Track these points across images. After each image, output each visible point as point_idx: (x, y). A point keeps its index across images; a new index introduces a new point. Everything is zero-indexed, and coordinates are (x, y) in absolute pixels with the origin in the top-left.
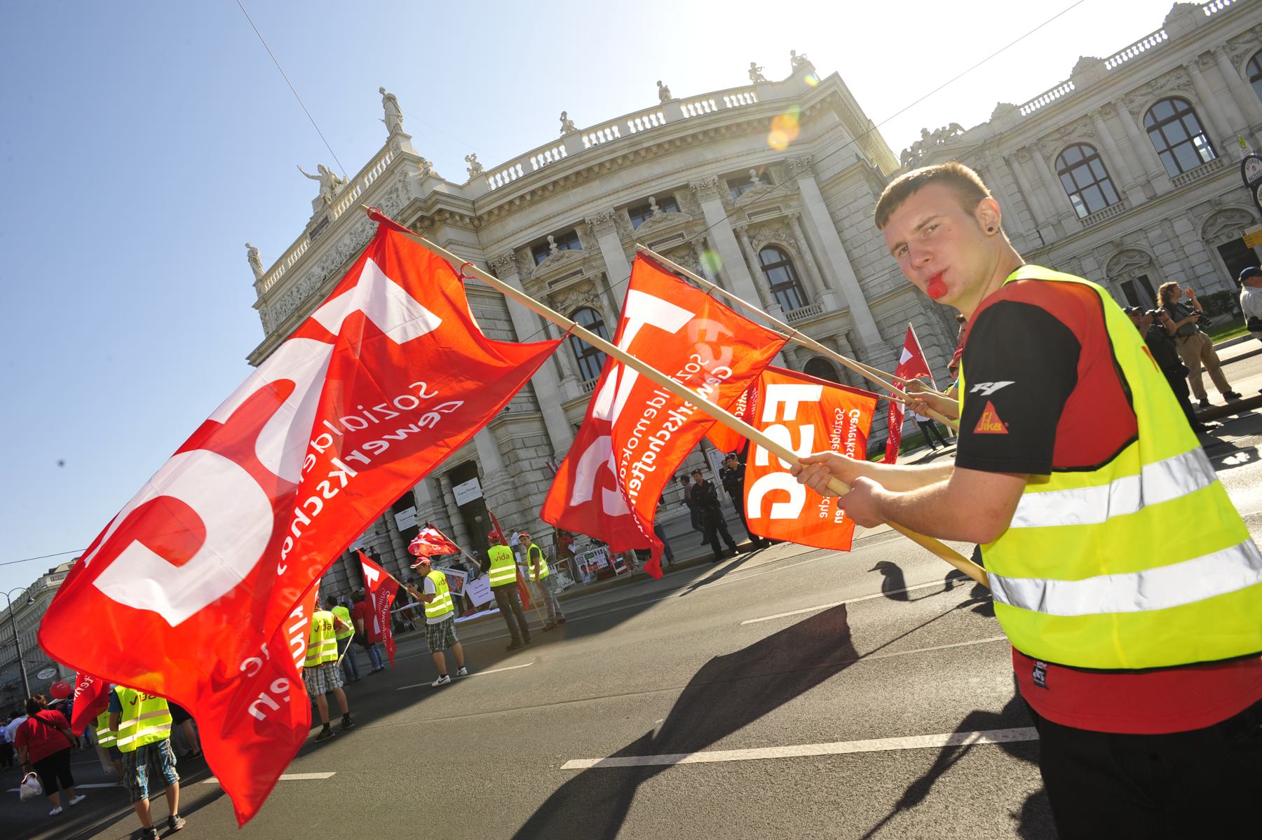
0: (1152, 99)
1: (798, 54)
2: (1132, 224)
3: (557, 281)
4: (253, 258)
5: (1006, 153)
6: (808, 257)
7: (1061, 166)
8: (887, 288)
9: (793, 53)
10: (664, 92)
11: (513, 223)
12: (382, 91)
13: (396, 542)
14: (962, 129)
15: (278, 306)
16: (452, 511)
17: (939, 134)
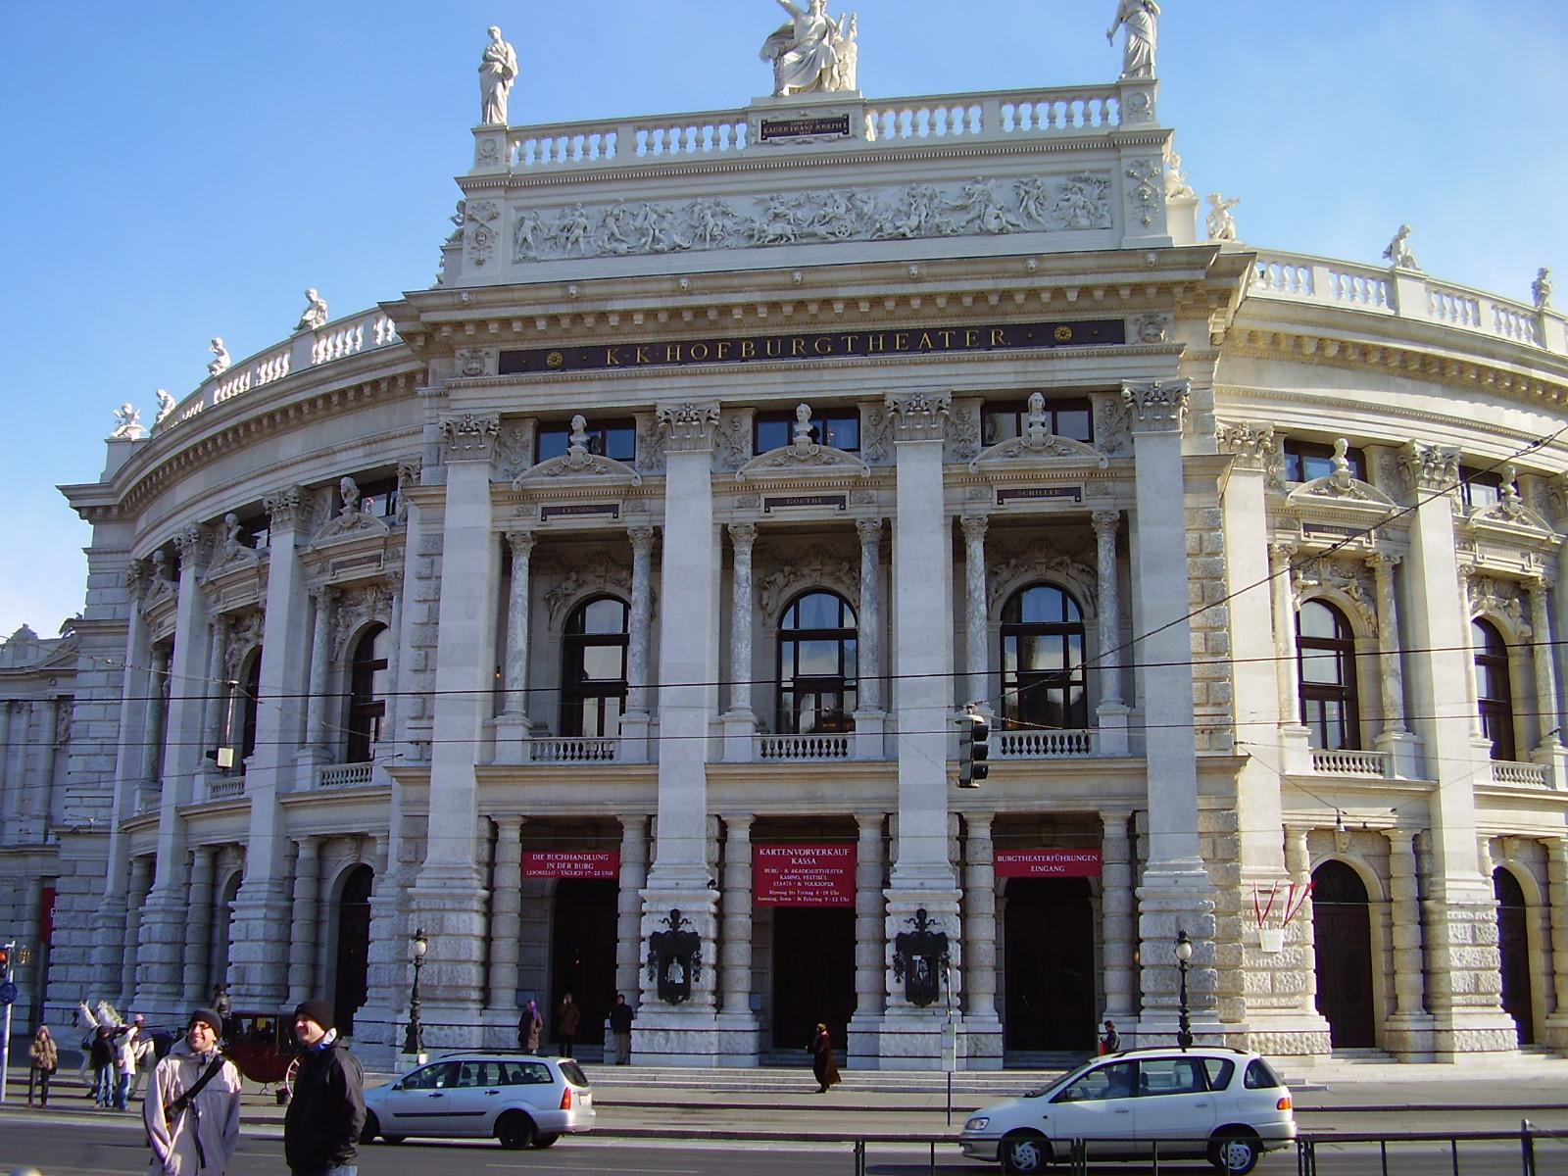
13: (741, 921)
15: (550, 220)
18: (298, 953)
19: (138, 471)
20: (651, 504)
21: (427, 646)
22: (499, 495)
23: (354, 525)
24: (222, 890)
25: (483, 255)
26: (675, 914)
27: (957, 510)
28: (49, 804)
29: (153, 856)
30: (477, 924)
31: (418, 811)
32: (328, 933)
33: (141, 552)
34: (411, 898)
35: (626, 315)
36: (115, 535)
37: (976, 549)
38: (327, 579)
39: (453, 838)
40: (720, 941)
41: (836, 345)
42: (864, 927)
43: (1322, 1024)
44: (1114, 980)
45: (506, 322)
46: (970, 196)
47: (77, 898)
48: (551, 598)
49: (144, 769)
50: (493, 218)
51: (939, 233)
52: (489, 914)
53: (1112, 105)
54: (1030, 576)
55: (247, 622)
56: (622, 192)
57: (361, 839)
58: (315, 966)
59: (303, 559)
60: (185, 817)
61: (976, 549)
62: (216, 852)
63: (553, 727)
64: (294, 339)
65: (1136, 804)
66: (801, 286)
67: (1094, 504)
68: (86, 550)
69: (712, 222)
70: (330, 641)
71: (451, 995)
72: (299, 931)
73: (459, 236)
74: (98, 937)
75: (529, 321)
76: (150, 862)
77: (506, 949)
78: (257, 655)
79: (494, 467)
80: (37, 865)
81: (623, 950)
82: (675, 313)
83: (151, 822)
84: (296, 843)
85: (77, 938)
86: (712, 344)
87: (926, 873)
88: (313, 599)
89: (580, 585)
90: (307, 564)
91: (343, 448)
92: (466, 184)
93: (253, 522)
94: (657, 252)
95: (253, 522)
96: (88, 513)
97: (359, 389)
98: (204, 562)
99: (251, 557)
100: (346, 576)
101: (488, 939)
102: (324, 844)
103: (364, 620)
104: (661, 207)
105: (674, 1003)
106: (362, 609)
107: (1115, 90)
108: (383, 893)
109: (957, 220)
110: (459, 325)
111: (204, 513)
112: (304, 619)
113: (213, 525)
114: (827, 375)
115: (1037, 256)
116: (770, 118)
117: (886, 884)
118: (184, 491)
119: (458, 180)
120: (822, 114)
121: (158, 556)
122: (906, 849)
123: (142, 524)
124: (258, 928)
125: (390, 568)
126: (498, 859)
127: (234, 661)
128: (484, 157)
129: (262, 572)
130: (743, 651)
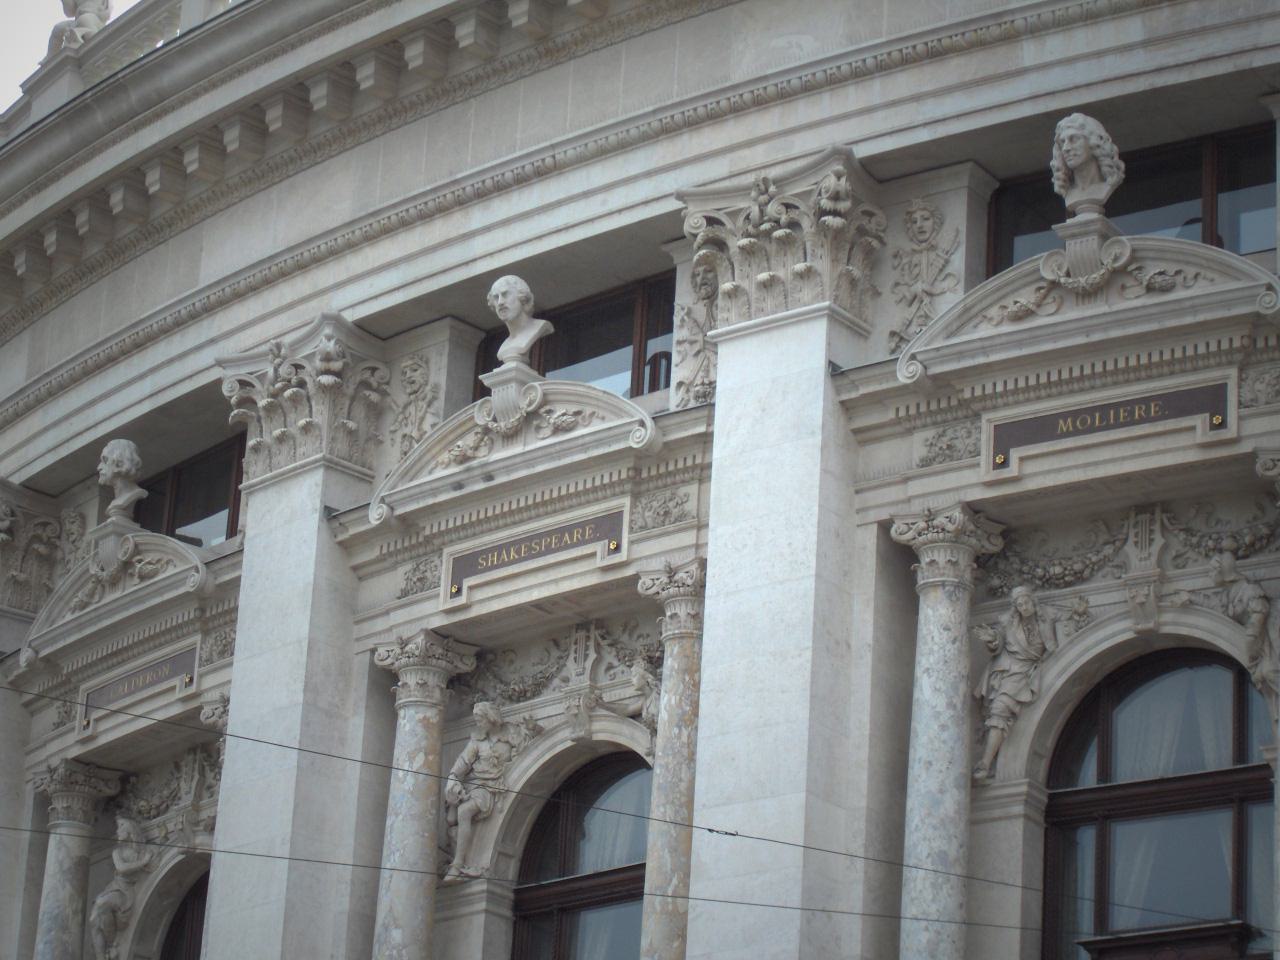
23: (1116, 279)
38: (972, 481)
55: (526, 669)
59: (859, 407)
88: (900, 562)
90: (862, 437)
93: (614, 306)
95: (614, 306)
100: (1044, 470)
103: (1112, 633)
106: (1102, 594)
111: (371, 284)
112: (864, 619)
121: (119, 455)
127: (478, 798)
129: (671, 469)
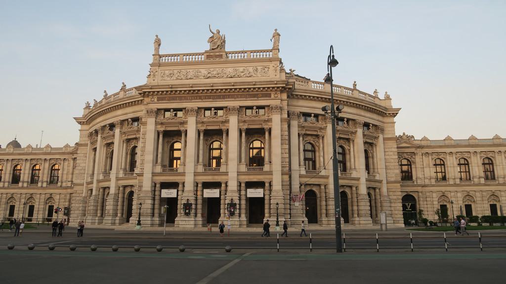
0: (461, 156)
1: (388, 94)
2: (449, 189)
3: (308, 130)
4: (158, 43)
5: (423, 152)
6: (375, 159)
7: (435, 163)
8: (393, 180)
9: (386, 93)
10: (355, 85)
11: (302, 103)
12: (276, 30)
13: (200, 201)
14: (414, 138)
15: (167, 72)
16: (243, 198)
17: (407, 136)
18: (119, 207)
19: (89, 115)
20: (185, 126)
21: (143, 151)
22: (156, 123)
24: (105, 196)
25: (155, 79)
26: (188, 200)
27: (240, 127)
28: (72, 178)
29: (92, 189)
30: (150, 202)
31: (141, 181)
32: (126, 203)
33: (91, 130)
34: (140, 197)
35: (181, 91)
36: (86, 127)
37: (244, 134)
38: (126, 138)
39: (147, 186)
40: (196, 204)
41: (219, 97)
42: (222, 202)
43: (306, 219)
44: (266, 211)
45: (158, 92)
46: (244, 70)
47: (77, 198)
48: (168, 142)
49: (91, 172)
50: (157, 72)
51: (239, 77)
52: (154, 199)
53: (271, 53)
54: (255, 139)
56: (180, 67)
57: (132, 186)
58: (123, 210)
59: (122, 133)
60: (99, 181)
61: (244, 134)
62: (104, 188)
63: (168, 166)
64: (119, 92)
65: (271, 180)
66: (212, 86)
67: (266, 127)
68: (80, 130)
69: (196, 73)
70: (127, 149)
71: (146, 214)
72: (120, 203)
73: (150, 75)
74: (81, 205)
75: (163, 92)
76: (92, 190)
77: (157, 206)
78: (113, 151)
79: (156, 118)
80: (69, 191)
81: (179, 206)
82: (190, 91)
83: (92, 183)
84: (119, 187)
85: (77, 205)
86: (197, 96)
87: (232, 193)
88: (123, 141)
89: (173, 140)
91: (129, 113)
92: (151, 65)
93: (112, 126)
94: (187, 79)
96: (80, 123)
97: (132, 102)
98: (102, 133)
99: (111, 133)
100: (129, 137)
101: (154, 204)
102: (125, 187)
103: (133, 145)
104: (188, 70)
105: (188, 216)
107: (271, 51)
108: (135, 196)
109: (242, 74)
110: (149, 92)
111: (103, 124)
113: (105, 126)
114: (217, 103)
115: (256, 82)
116: (208, 54)
117: (226, 194)
118: (98, 120)
119: (150, 64)
120: (218, 54)
122: (229, 188)
123: (91, 125)
124: (112, 203)
125: (138, 136)
126: (156, 190)
128: (155, 60)
129: (114, 136)
130: (201, 152)
